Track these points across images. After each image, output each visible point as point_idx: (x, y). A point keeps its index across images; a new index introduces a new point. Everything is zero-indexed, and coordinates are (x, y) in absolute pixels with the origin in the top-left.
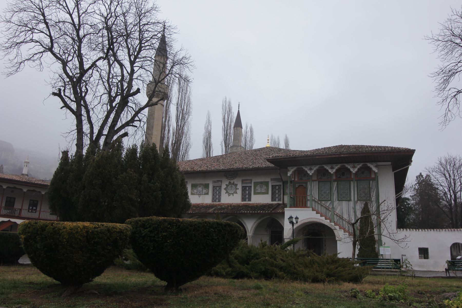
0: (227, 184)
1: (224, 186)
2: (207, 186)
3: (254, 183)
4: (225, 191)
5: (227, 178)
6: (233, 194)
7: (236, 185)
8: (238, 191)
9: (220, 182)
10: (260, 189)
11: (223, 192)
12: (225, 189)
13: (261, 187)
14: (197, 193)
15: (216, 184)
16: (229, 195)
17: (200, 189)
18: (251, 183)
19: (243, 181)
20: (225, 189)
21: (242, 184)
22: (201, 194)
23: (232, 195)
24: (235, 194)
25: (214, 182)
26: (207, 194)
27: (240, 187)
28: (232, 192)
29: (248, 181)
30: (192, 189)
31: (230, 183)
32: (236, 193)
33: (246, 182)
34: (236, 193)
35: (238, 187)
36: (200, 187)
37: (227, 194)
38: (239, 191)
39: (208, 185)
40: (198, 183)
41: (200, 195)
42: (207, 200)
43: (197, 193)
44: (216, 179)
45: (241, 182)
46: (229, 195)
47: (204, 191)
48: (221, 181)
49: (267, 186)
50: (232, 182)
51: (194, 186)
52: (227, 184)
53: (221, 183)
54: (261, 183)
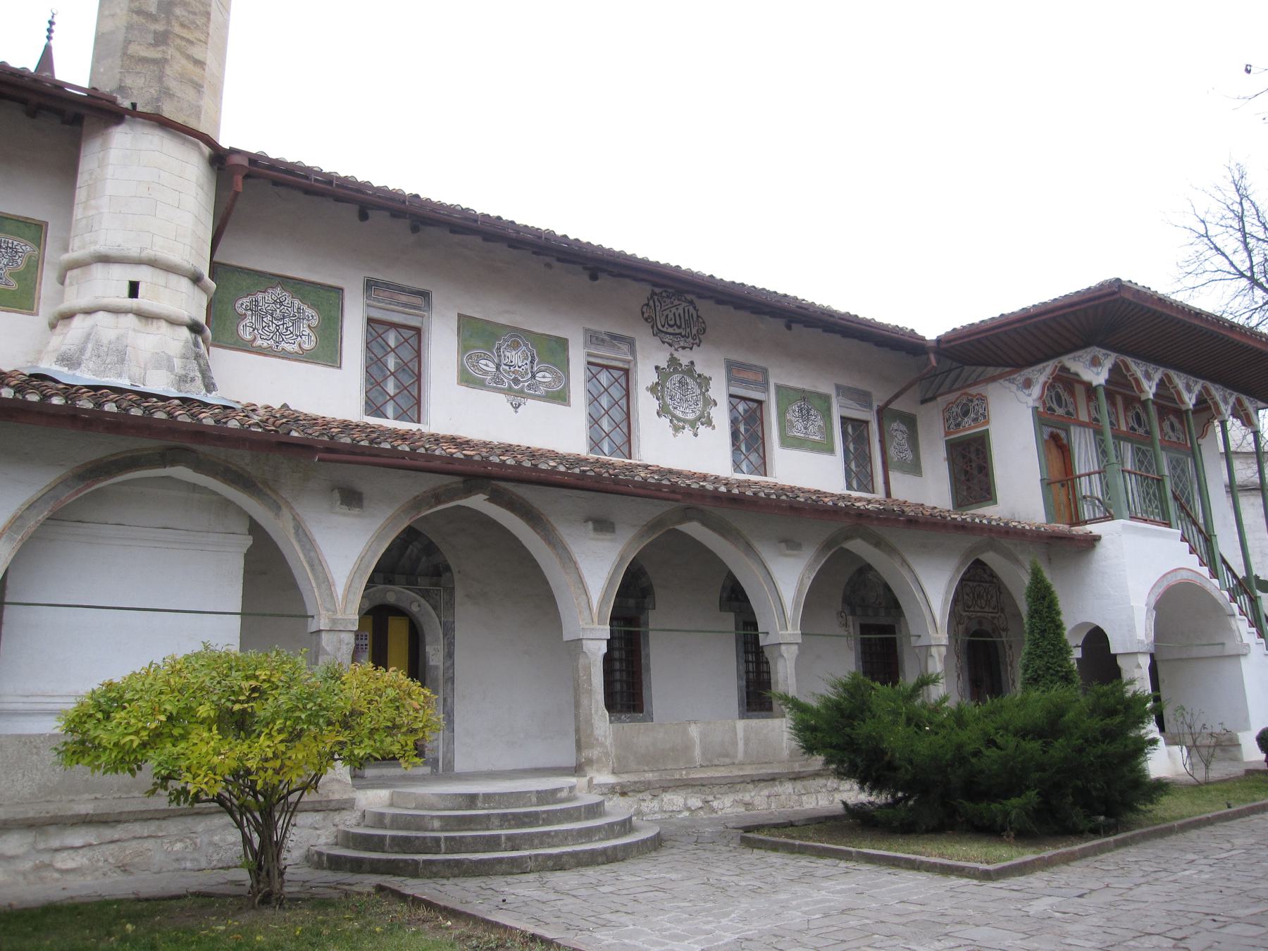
0: (663, 364)
1: (645, 376)
2: (555, 350)
3: (778, 387)
4: (655, 404)
5: (658, 332)
6: (693, 424)
7: (704, 382)
8: (714, 412)
9: (625, 348)
10: (800, 426)
11: (645, 404)
12: (653, 389)
13: (805, 415)
14: (497, 380)
15: (606, 354)
16: (677, 429)
17: (515, 357)
18: (765, 386)
19: (734, 370)
20: (653, 389)
21: (731, 380)
22: (520, 393)
23: (688, 432)
24: (702, 429)
25: (593, 338)
26: (561, 397)
27: (719, 390)
28: (691, 416)
29: (750, 376)
30: (464, 348)
31: (673, 361)
32: (709, 423)
33: (743, 375)
34: (709, 423)
35: (712, 393)
36: (515, 346)
37: (665, 421)
38: (721, 416)
39: (563, 343)
40: (503, 320)
41: (517, 394)
42: (555, 429)
43: (497, 380)
44: (604, 327)
45: (723, 372)
46: (677, 429)
47: (544, 377)
48: (631, 343)
49: (827, 414)
50: (684, 358)
51: (476, 335)
52: (663, 364)
53: (633, 352)
54: (804, 396)
